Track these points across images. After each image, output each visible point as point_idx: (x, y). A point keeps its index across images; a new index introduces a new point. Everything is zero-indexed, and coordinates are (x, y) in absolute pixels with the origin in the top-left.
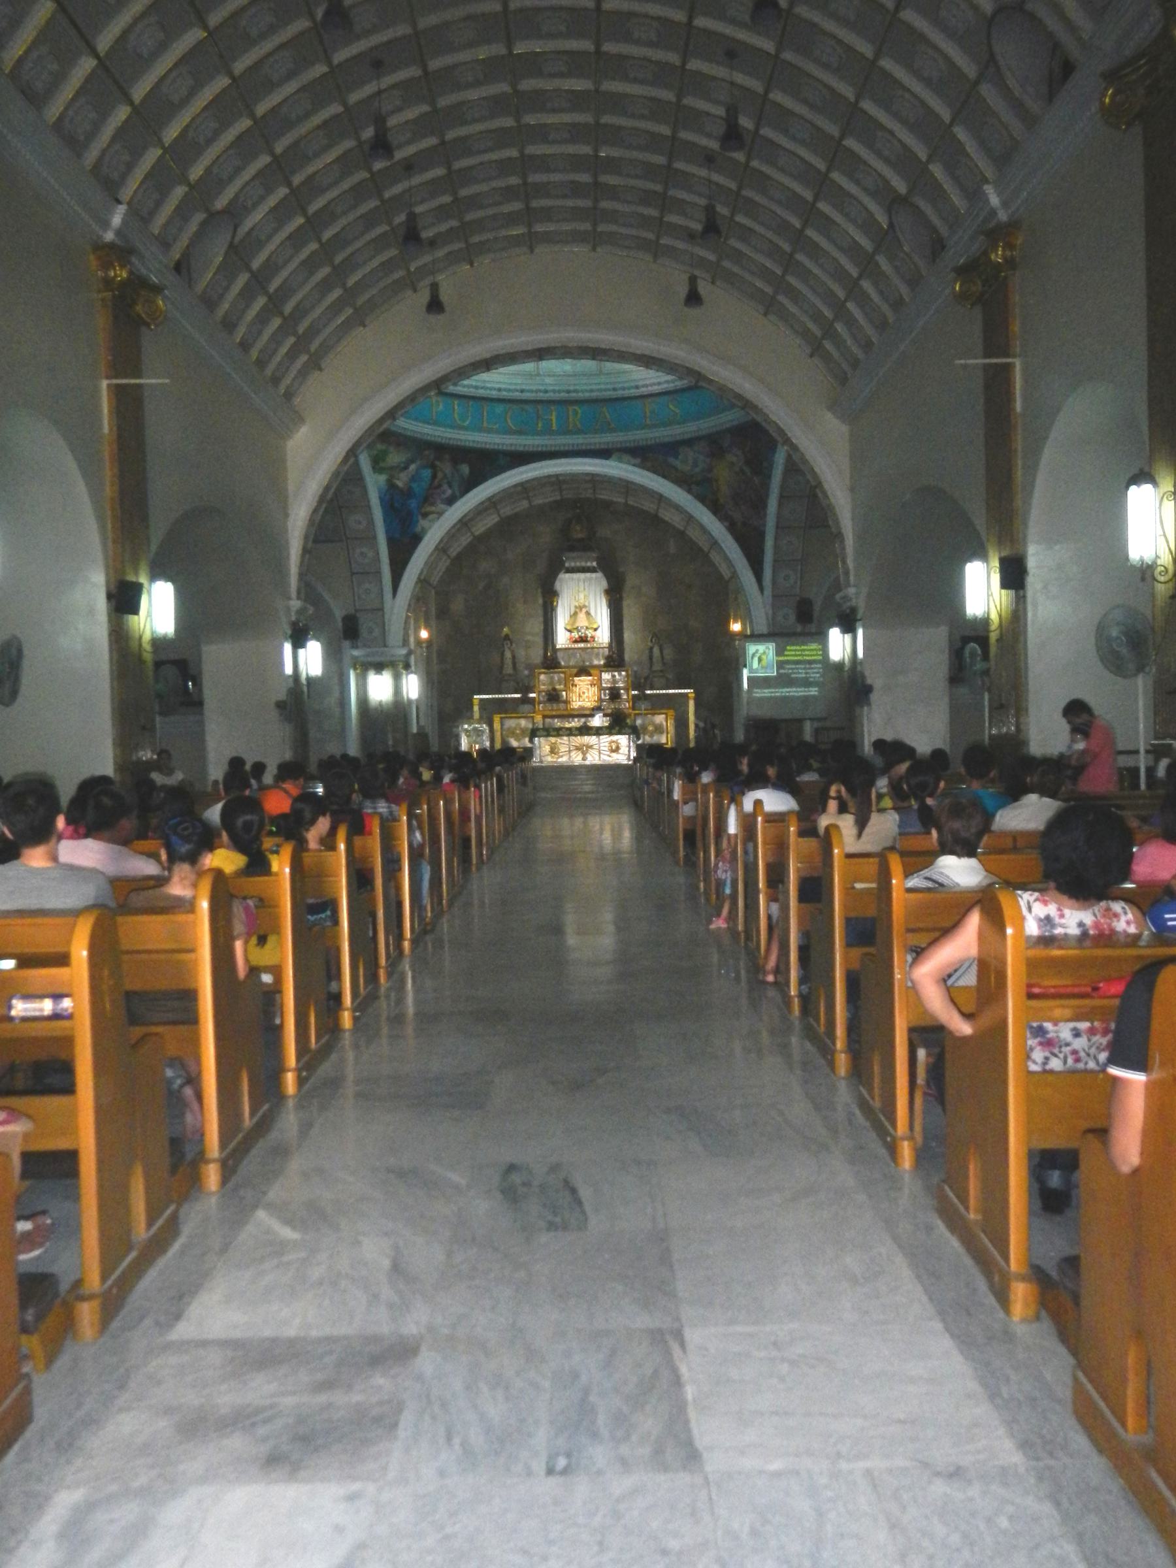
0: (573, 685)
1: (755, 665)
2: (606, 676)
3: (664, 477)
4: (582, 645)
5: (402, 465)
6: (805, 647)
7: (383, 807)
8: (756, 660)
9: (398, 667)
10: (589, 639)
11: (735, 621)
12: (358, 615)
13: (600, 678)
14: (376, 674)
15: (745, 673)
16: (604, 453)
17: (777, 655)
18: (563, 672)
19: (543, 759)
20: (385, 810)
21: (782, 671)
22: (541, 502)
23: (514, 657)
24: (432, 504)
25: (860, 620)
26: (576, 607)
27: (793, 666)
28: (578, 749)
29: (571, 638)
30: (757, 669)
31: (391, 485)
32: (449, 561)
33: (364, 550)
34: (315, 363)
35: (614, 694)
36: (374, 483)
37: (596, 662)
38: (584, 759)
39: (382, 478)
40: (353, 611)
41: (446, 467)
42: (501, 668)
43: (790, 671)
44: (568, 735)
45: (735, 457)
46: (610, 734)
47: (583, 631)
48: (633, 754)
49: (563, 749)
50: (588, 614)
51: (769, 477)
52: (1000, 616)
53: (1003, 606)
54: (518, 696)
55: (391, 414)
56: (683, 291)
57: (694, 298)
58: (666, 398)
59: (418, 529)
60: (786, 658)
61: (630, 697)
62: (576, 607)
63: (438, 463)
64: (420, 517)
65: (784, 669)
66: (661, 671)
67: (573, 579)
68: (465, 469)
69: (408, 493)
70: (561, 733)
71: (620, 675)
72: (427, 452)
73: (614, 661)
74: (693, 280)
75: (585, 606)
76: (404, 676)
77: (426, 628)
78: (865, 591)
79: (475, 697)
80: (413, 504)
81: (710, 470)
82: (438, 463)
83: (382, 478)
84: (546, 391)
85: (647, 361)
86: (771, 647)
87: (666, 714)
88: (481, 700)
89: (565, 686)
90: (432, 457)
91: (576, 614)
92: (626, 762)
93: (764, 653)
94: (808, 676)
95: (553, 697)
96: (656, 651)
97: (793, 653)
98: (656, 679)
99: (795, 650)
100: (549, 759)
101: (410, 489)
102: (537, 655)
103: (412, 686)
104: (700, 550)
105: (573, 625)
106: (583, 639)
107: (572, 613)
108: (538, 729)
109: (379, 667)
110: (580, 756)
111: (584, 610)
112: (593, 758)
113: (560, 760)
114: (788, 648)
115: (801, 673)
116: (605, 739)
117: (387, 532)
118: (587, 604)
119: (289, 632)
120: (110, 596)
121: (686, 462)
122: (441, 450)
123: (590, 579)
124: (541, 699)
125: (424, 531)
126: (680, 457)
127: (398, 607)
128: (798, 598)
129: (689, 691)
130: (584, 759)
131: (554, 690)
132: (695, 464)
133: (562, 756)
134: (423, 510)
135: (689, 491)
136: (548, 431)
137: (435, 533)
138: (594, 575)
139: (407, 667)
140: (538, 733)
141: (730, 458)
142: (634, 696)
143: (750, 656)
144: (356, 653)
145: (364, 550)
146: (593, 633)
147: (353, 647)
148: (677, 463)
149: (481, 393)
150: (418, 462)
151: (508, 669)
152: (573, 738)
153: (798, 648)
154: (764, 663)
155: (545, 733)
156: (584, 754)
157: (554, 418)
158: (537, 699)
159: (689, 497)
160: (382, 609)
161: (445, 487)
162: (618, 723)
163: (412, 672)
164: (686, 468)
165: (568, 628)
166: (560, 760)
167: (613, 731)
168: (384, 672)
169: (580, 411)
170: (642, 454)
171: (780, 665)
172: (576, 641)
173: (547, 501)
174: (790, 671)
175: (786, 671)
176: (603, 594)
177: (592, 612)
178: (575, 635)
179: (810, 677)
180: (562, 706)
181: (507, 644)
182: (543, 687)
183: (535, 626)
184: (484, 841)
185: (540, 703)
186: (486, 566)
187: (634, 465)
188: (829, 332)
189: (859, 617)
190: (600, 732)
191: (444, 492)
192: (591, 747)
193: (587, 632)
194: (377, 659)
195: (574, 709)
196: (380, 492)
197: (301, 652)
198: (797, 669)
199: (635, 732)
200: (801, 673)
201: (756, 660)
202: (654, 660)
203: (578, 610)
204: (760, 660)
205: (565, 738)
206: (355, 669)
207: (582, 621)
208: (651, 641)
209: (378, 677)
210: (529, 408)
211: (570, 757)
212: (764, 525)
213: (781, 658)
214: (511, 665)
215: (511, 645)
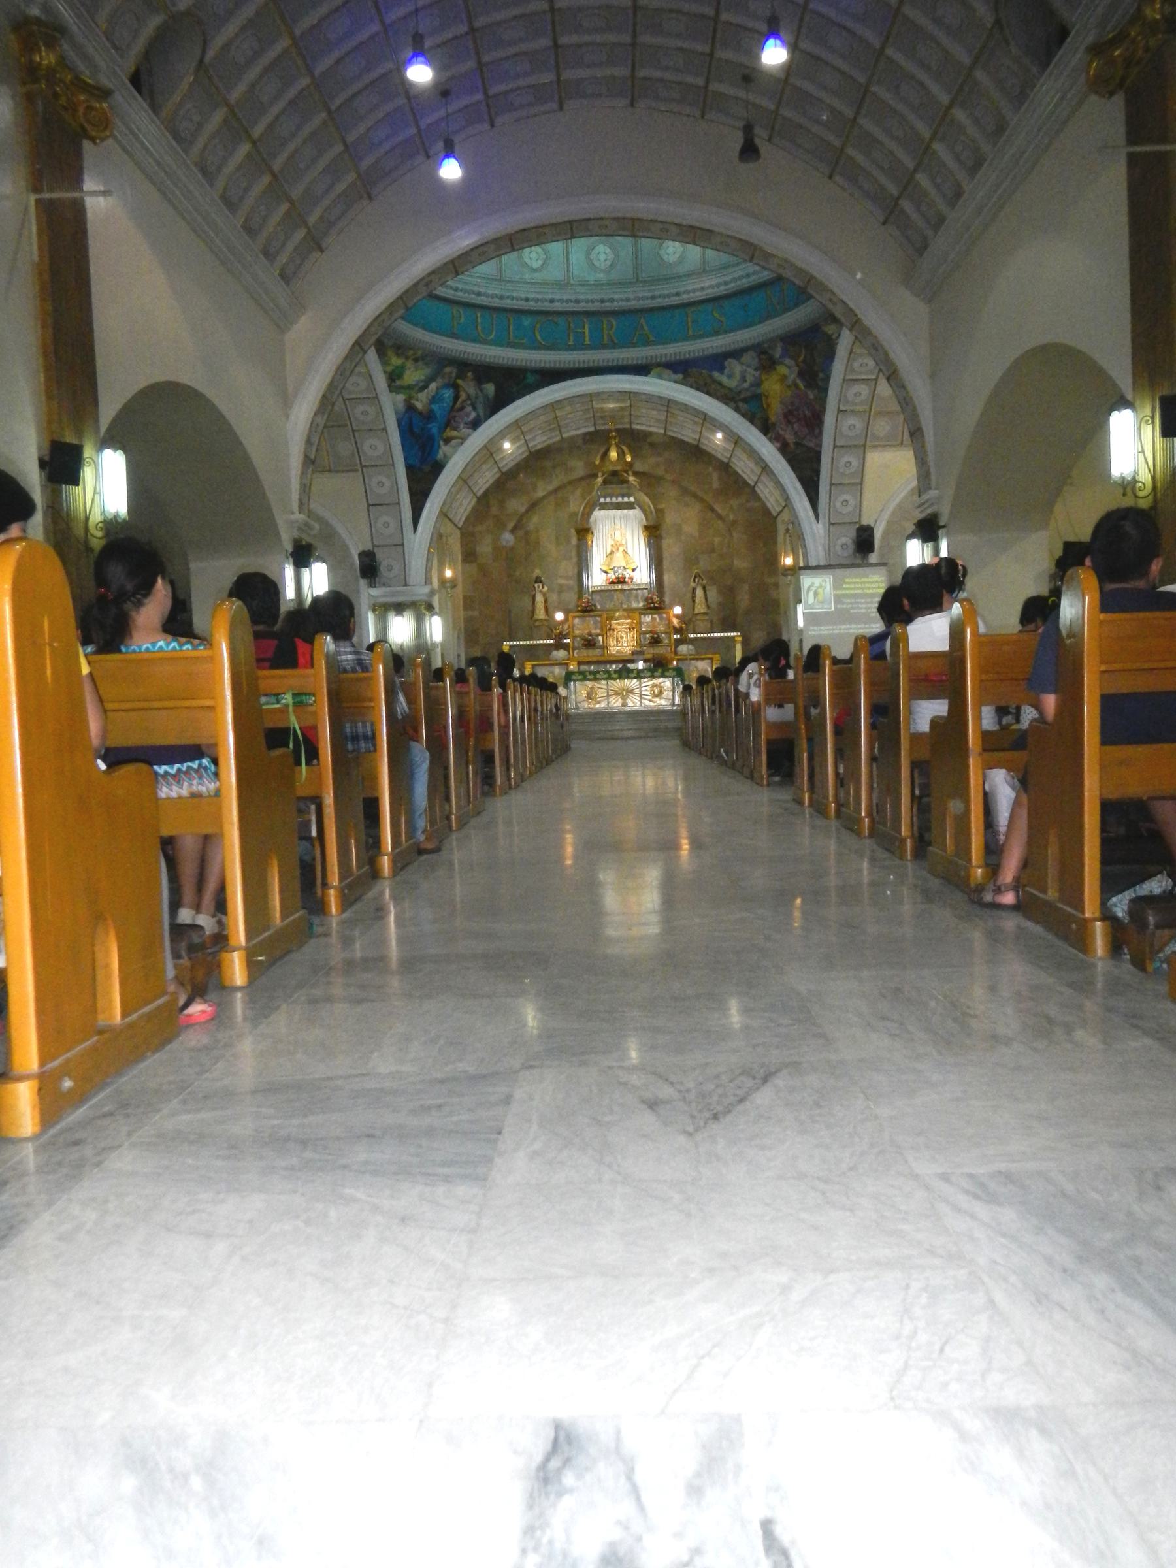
0: (610, 629)
1: (811, 600)
2: (648, 619)
3: (708, 393)
4: (620, 587)
5: (421, 384)
6: (866, 580)
7: (346, 653)
8: (811, 594)
9: (421, 609)
10: (626, 579)
11: (786, 555)
12: (376, 550)
13: (640, 623)
14: (396, 615)
15: (800, 609)
16: (642, 369)
17: (835, 588)
18: (600, 616)
19: (579, 705)
20: (350, 657)
21: (839, 606)
22: (573, 433)
23: (546, 601)
24: (456, 429)
25: (944, 527)
26: (612, 545)
27: (853, 601)
28: (617, 693)
29: (607, 580)
30: (813, 604)
31: (410, 408)
32: (475, 500)
33: (384, 480)
34: (315, 243)
35: (656, 641)
36: (390, 405)
37: (635, 605)
38: (624, 705)
39: (401, 397)
40: (371, 548)
41: (469, 387)
42: (533, 612)
43: (850, 606)
44: (606, 679)
45: (787, 370)
46: (652, 677)
47: (620, 571)
48: (677, 701)
49: (601, 693)
50: (625, 552)
51: (825, 390)
52: (1153, 478)
53: (1158, 468)
54: (552, 641)
55: (404, 304)
56: (737, 141)
57: (749, 151)
58: (710, 307)
59: (440, 456)
60: (844, 592)
61: (672, 641)
62: (612, 545)
63: (459, 381)
64: (442, 443)
65: (843, 604)
66: (705, 614)
67: (608, 517)
68: (490, 388)
69: (429, 416)
70: (598, 676)
71: (661, 618)
72: (448, 370)
73: (653, 603)
74: (748, 130)
75: (621, 545)
76: (427, 618)
77: (450, 568)
78: (950, 492)
79: (505, 643)
80: (434, 428)
81: (758, 383)
82: (459, 381)
83: (401, 397)
84: (577, 301)
85: (692, 234)
86: (827, 580)
87: (712, 659)
89: (602, 630)
90: (454, 375)
91: (612, 553)
92: (669, 707)
93: (821, 586)
94: (869, 610)
95: (590, 643)
96: (699, 592)
97: (852, 586)
98: (698, 622)
99: (855, 583)
100: (586, 705)
101: (431, 411)
102: (571, 597)
103: (436, 629)
104: (746, 483)
105: (608, 565)
106: (621, 581)
107: (608, 553)
108: (573, 673)
109: (399, 608)
110: (619, 703)
111: (621, 549)
112: (633, 703)
113: (597, 706)
114: (847, 580)
115: (861, 608)
116: (647, 683)
117: (406, 459)
118: (624, 542)
119: (289, 548)
120: (42, 464)
121: (735, 375)
122: (464, 366)
123: (627, 518)
124: (576, 645)
125: (447, 458)
126: (726, 371)
127: (419, 541)
128: (857, 526)
129: (736, 634)
130: (624, 705)
131: (590, 634)
132: (744, 379)
133: (599, 702)
134: (445, 435)
135: (737, 410)
136: (580, 346)
137: (457, 460)
138: (631, 512)
139: (430, 608)
140: (574, 677)
141: (782, 370)
142: (676, 640)
143: (806, 588)
144: (374, 592)
145: (384, 480)
146: (632, 574)
147: (372, 584)
148: (724, 379)
149: (508, 303)
150: (440, 380)
151: (541, 614)
152: (612, 681)
153: (857, 580)
154: (820, 597)
155: (580, 677)
156: (624, 699)
157: (587, 331)
158: (571, 645)
159: (736, 415)
160: (403, 545)
161: (469, 409)
162: (658, 666)
163: (436, 614)
164: (731, 383)
165: (605, 568)
166: (597, 706)
167: (656, 674)
168: (405, 614)
169: (614, 323)
170: (682, 369)
171: (838, 599)
172: (613, 583)
173: (579, 432)
174: (850, 606)
175: (845, 606)
176: (641, 532)
177: (629, 551)
178: (612, 576)
179: (870, 612)
180: (598, 652)
181: (539, 587)
182: (577, 632)
183: (567, 568)
184: (512, 761)
185: (574, 649)
186: (517, 505)
187: (675, 382)
188: (908, 185)
189: (942, 524)
190: (643, 675)
191: (468, 415)
192: (631, 692)
193: (625, 573)
194: (400, 599)
195: (612, 655)
196: (396, 413)
197: (305, 572)
198: (858, 603)
199: (679, 673)
200: (861, 608)
201: (811, 594)
202: (697, 601)
203: (614, 550)
204: (816, 594)
205: (604, 682)
206: (374, 610)
207: (619, 560)
209: (399, 618)
210: (561, 321)
211: (608, 703)
212: (820, 446)
213: (839, 592)
214: (543, 611)
215: (543, 587)
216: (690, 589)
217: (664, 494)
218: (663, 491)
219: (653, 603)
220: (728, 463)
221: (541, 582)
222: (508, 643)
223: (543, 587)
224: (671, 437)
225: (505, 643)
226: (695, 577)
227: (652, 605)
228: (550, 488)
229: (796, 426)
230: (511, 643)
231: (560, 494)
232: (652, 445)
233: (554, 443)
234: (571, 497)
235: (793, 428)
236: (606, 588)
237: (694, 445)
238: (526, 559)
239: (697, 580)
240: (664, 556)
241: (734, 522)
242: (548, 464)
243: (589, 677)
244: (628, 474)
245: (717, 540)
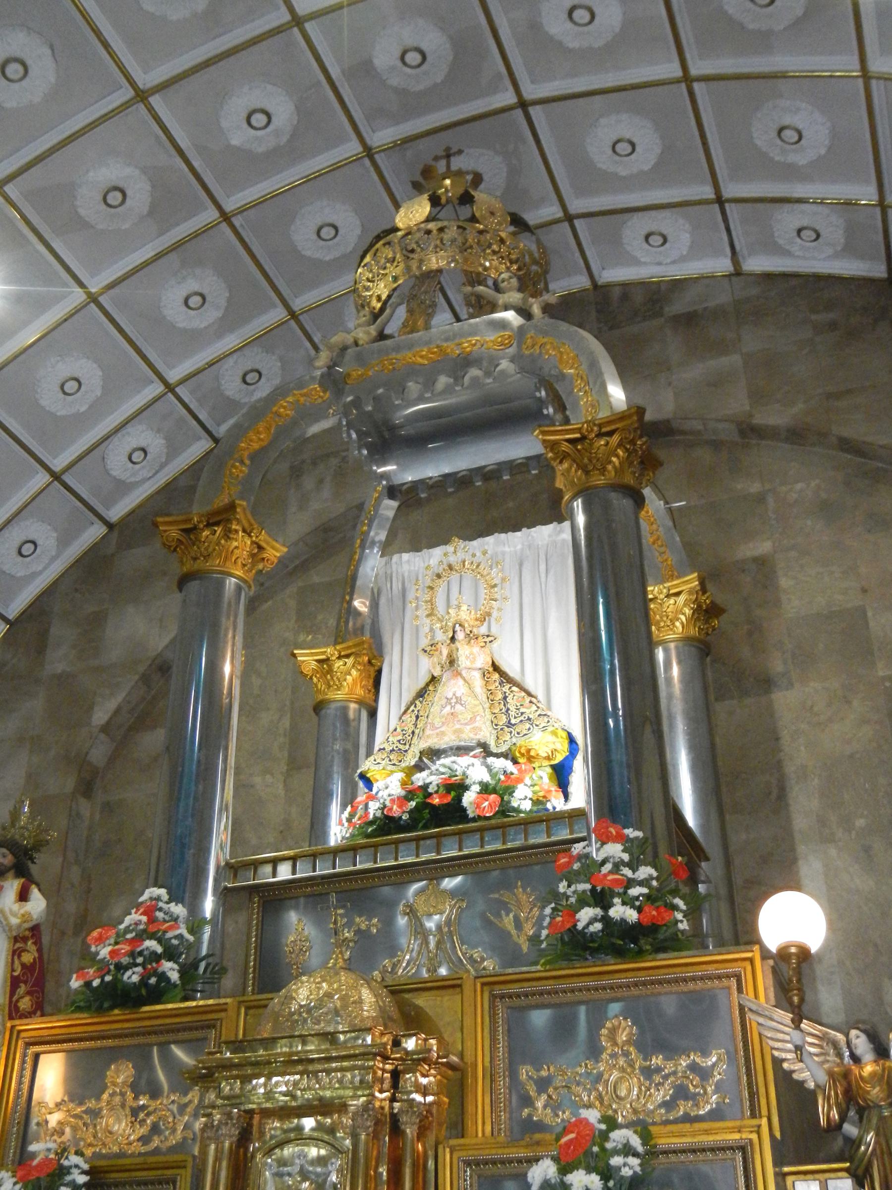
215: (23, 896)
217: (761, 499)
218: (755, 487)
219: (602, 899)
223: (23, 896)
224: (768, 277)
227: (586, 914)
232: (689, 320)
240: (790, 769)
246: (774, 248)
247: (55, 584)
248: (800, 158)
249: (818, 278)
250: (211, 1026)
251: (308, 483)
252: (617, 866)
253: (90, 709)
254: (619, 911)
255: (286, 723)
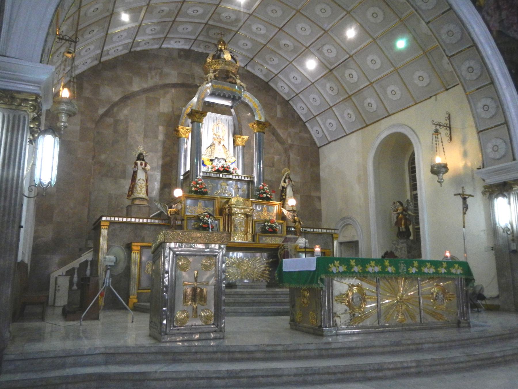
10: (231, 170)
42: (132, 189)
79: (104, 218)
88: (111, 223)
138: (224, 117)
172: (218, 171)
203: (216, 143)
208: (285, 182)
214: (144, 189)
215: (146, 165)
216: (280, 188)
220: (288, 101)
221: (143, 160)
222: (108, 219)
224: (249, 72)
225: (104, 218)
226: (286, 178)
227: (265, 195)
228: (145, 86)
229: (504, 13)
230: (112, 219)
231: (151, 95)
233: (152, 50)
234: (161, 99)
235: (500, 15)
236: (212, 175)
237: (263, 81)
238: (113, 145)
239: (287, 181)
241: (291, 146)
242: (144, 65)
243: (356, 269)
244: (236, 77)
245: (276, 157)
246: (253, 68)
247: (84, 72)
248: (270, 63)
249: (258, 77)
250: (215, 199)
251: (153, 73)
252: (266, 189)
253: (98, 109)
254: (268, 196)
255: (143, 126)
